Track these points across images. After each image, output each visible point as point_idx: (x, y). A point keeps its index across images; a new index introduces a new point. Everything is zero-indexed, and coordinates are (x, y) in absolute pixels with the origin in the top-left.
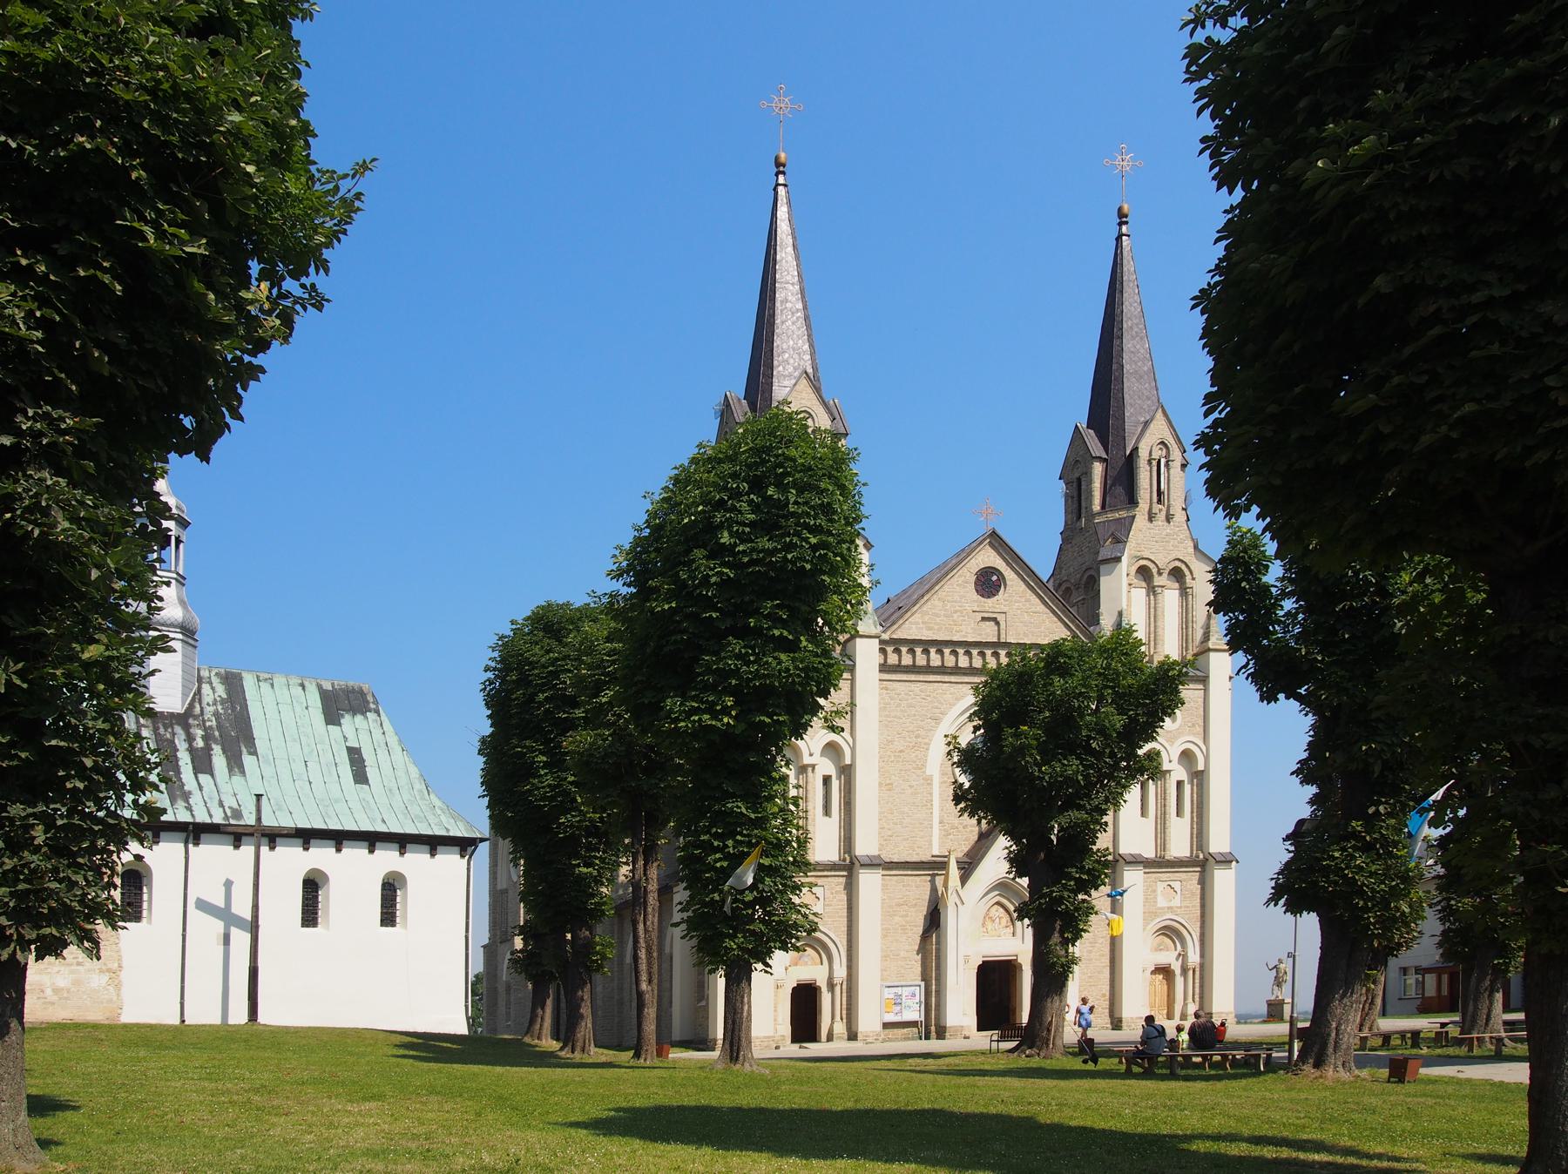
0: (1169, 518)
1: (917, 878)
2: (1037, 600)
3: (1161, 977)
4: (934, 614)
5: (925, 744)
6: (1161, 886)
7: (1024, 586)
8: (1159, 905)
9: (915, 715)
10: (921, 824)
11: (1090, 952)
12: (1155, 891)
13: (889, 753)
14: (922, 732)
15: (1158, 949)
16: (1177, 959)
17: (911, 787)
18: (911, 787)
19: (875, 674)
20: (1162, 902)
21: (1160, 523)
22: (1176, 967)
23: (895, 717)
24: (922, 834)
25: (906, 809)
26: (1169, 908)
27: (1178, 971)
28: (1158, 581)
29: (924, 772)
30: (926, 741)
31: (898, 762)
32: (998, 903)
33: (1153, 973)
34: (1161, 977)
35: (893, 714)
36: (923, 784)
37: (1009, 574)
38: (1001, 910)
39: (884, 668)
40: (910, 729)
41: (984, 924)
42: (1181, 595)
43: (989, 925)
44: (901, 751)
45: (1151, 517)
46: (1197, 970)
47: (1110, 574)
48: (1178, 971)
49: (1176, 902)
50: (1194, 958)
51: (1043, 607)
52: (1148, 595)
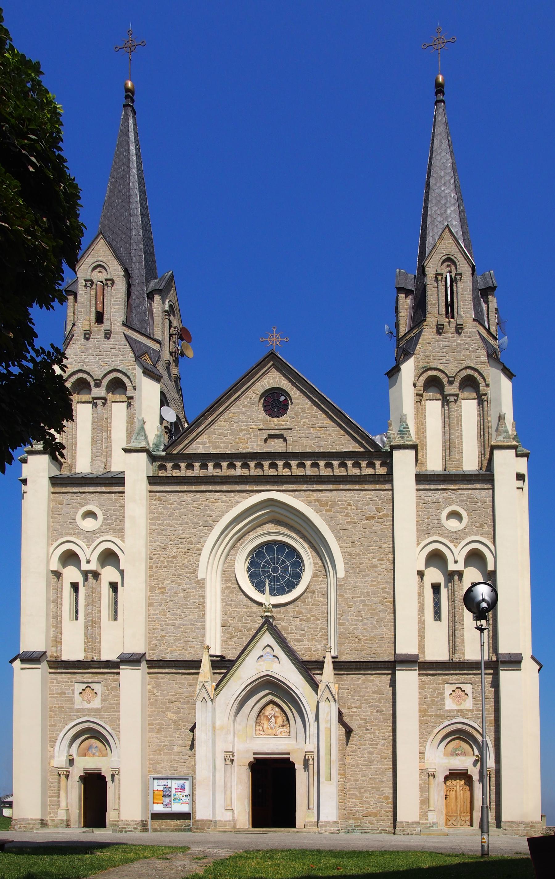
0: (459, 329)
1: (189, 676)
2: (324, 415)
3: (463, 782)
4: (222, 434)
5: (197, 549)
6: (448, 689)
7: (309, 403)
8: (447, 708)
9: (187, 523)
10: (194, 625)
11: (371, 753)
12: (442, 693)
13: (162, 559)
14: (194, 539)
15: (455, 754)
16: (475, 764)
17: (184, 590)
18: (184, 590)
19: (144, 485)
20: (450, 705)
21: (450, 335)
22: (474, 772)
23: (168, 525)
24: (195, 634)
25: (179, 612)
26: (458, 711)
27: (476, 777)
28: (450, 390)
29: (196, 576)
30: (199, 546)
31: (172, 567)
32: (272, 702)
33: (447, 778)
34: (463, 782)
35: (165, 523)
36: (195, 588)
37: (294, 393)
38: (277, 709)
39: (152, 480)
40: (183, 536)
41: (258, 723)
42: (479, 404)
43: (266, 725)
44: (174, 557)
45: (440, 329)
46: (493, 776)
47: (395, 385)
48: (476, 777)
49: (468, 704)
50: (491, 763)
51: (329, 421)
52: (443, 406)
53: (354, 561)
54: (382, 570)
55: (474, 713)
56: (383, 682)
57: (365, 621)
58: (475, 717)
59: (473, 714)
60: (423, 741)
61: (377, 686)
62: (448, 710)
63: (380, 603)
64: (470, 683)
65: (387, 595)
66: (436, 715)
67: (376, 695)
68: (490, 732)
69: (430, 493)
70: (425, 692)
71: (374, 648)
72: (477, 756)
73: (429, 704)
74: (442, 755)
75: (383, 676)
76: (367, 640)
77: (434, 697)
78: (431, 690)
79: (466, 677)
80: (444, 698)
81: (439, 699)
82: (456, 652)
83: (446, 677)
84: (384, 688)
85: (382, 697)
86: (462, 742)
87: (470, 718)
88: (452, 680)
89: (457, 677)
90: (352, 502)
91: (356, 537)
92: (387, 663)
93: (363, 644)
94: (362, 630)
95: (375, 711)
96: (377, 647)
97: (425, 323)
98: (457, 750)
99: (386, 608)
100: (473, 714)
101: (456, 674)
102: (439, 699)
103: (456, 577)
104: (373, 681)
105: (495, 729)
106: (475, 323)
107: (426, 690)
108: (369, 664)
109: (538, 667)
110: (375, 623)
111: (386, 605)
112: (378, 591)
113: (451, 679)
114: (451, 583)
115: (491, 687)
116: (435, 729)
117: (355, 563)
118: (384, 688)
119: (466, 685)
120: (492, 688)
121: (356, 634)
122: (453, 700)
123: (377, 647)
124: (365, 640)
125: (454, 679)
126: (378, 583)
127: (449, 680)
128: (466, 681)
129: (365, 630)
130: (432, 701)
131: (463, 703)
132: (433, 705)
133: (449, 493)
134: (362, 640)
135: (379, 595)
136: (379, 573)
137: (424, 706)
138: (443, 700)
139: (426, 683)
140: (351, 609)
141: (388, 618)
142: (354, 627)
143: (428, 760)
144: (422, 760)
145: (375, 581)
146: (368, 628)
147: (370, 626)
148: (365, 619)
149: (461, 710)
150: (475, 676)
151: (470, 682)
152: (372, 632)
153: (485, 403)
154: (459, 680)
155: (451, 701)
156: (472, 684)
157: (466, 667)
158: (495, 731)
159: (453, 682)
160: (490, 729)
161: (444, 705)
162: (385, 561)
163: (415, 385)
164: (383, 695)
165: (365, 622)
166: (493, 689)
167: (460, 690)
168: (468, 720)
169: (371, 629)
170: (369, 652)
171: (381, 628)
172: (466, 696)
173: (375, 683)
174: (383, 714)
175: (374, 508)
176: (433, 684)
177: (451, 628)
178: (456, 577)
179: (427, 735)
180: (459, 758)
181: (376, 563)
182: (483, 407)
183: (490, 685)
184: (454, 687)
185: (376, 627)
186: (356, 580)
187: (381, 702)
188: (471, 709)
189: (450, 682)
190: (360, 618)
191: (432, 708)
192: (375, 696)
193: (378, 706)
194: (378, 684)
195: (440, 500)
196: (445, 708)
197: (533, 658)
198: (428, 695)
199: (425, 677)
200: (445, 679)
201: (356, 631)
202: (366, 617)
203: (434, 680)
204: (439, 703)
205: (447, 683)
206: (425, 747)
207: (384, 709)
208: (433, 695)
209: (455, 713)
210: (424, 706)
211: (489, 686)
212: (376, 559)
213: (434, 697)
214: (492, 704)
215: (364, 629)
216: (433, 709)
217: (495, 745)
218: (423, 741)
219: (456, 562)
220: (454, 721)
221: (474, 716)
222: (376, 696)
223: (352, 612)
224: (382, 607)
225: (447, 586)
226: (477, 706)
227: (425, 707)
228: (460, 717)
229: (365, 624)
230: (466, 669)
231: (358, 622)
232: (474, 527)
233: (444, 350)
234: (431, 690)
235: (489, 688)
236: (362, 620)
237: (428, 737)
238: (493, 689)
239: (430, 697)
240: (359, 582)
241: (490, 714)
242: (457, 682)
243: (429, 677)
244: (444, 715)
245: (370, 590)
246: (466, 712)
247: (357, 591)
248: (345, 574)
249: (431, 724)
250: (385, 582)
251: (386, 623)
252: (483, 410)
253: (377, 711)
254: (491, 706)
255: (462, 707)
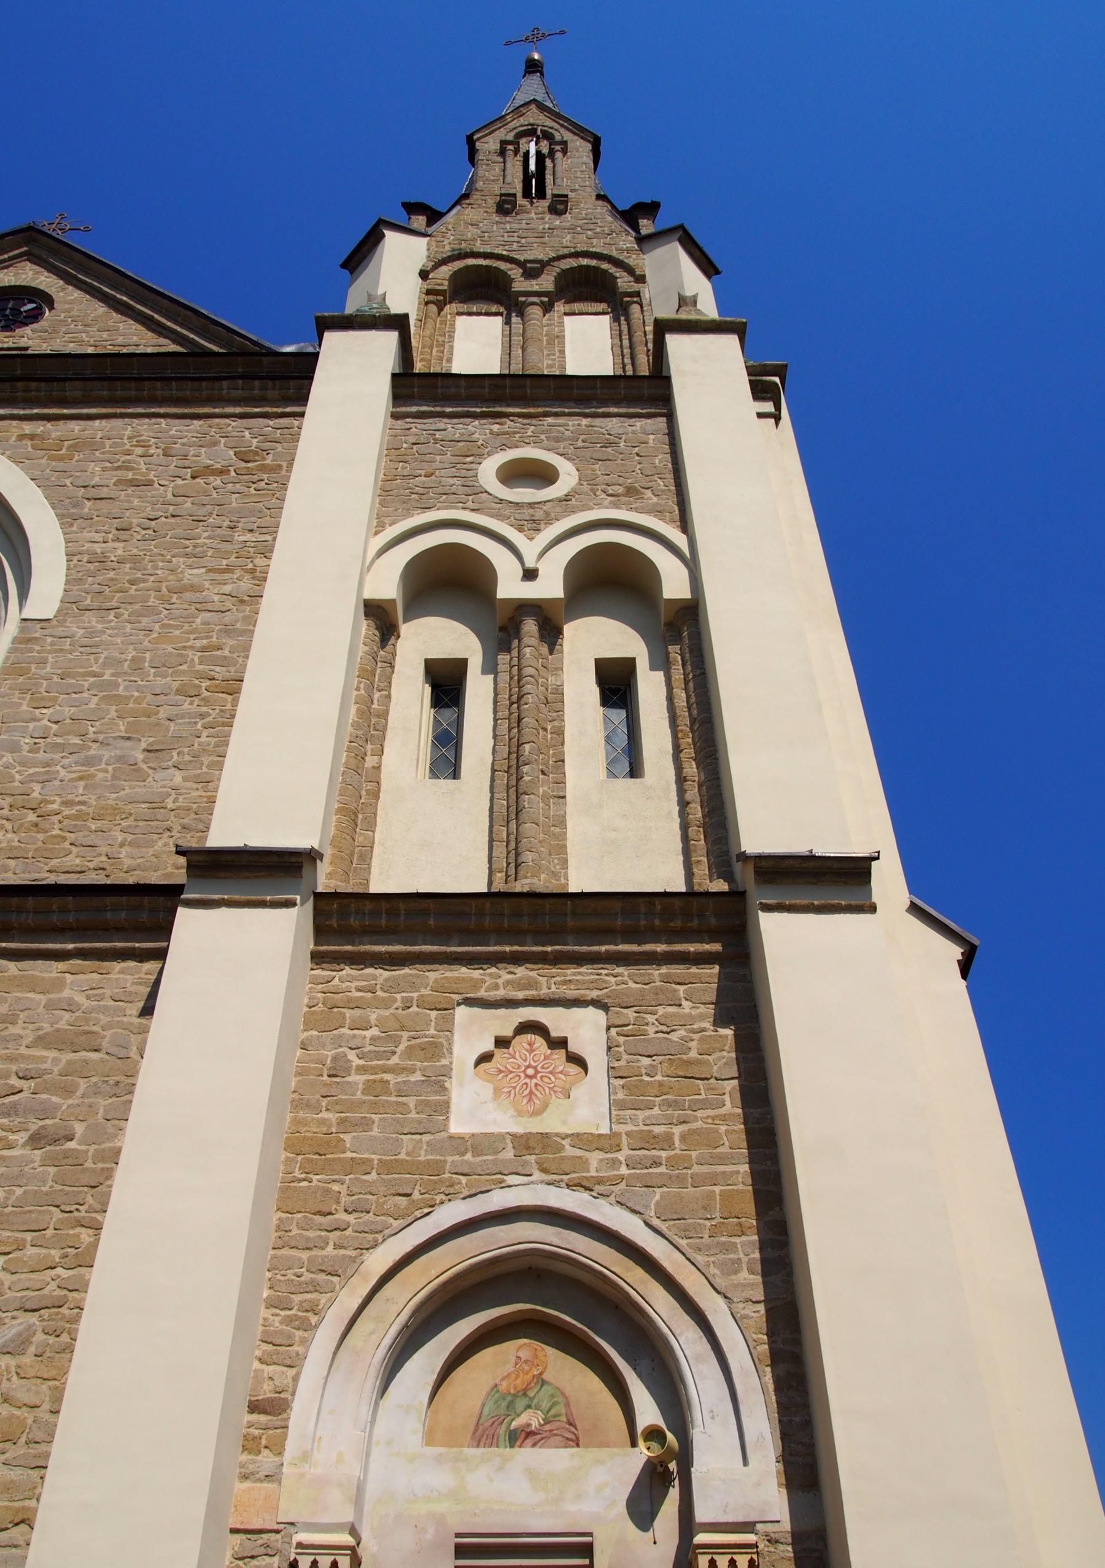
8: (456, 1127)
26: (525, 1143)
53: (112, 574)
54: (216, 598)
55: (621, 1156)
56: (108, 992)
57: (94, 750)
58: (630, 1182)
59: (615, 1163)
60: (288, 1321)
61: (70, 1007)
62: (461, 1138)
63: (179, 692)
64: (597, 1003)
65: (218, 669)
66: (387, 1167)
67: (52, 1054)
68: (733, 1267)
69: (441, 423)
70: (337, 1042)
71: (104, 850)
72: (654, 1434)
73: (359, 1105)
74: (412, 1431)
75: (118, 966)
76: (80, 816)
77: (386, 1070)
78: (374, 1031)
79: (571, 972)
80: (447, 1072)
81: (417, 1077)
82: (521, 873)
83: (463, 971)
84: (104, 1019)
85: (86, 1062)
86: (551, 1352)
87: (600, 1181)
88: (496, 987)
89: (521, 971)
90: (153, 440)
91: (144, 515)
92: (146, 900)
93: (56, 832)
94: (72, 780)
95: (21, 1137)
96: (122, 845)
97: (467, 201)
98: (521, 1403)
99: (204, 709)
100: (615, 1163)
101: (517, 959)
102: (417, 1077)
103: (530, 626)
104: (59, 985)
105: (763, 1246)
106: (600, 203)
107: (345, 1031)
108: (56, 903)
109: (956, 952)
110: (140, 756)
111: (203, 699)
112: (182, 655)
113: (489, 981)
114: (509, 651)
115: (720, 1020)
116: (375, 1246)
117: (112, 579)
118: (104, 1019)
119: (575, 1010)
120: (725, 1025)
121: (35, 795)
122: (497, 1092)
123: (122, 845)
124: (67, 817)
125: (508, 982)
126: (191, 633)
127: (477, 984)
128: (571, 993)
129: (82, 783)
130: (369, 1087)
131: (556, 1102)
132: (375, 1108)
133: (509, 422)
134: (55, 819)
135: (184, 667)
136: (202, 606)
137: (325, 1115)
138: (438, 1081)
139: (350, 1000)
140: (44, 711)
141: (203, 739)
142: (31, 771)
143: (305, 1457)
144: (266, 1460)
145: (177, 627)
146: (101, 775)
147: (110, 768)
148: (95, 746)
149: (545, 1136)
150: (620, 970)
151: (594, 994)
152: (117, 789)
153: (635, 309)
154: (531, 984)
155: (486, 1090)
156: (603, 1006)
157: (570, 922)
158: (764, 1261)
159: (501, 993)
160: (729, 1248)
161: (444, 1108)
162: (238, 573)
163: (424, 275)
164: (94, 1056)
165: (92, 752)
166: (728, 1032)
167: (539, 1042)
168: (585, 1196)
169: (114, 778)
170: (78, 861)
171: (159, 775)
172: (574, 1069)
173: (66, 993)
174: (67, 1154)
175: (232, 453)
176: (386, 1004)
177: (501, 794)
178: (530, 626)
179: (316, 1287)
180: (526, 1455)
181: (195, 581)
182: (628, 320)
183: (710, 1010)
184: (506, 1021)
185: (139, 770)
186: (100, 627)
187: (68, 1091)
188: (604, 1130)
189: (482, 993)
190: (76, 740)
191: (366, 1124)
192: (43, 1059)
193: (46, 1112)
194: (80, 998)
195: (476, 436)
196: (445, 1127)
197: (914, 909)
198: (352, 1056)
199: (348, 971)
200: (457, 980)
201: (37, 787)
202: (101, 737)
203: (391, 987)
204: (411, 1102)
205: (469, 1002)
206: (294, 1363)
207: (79, 1128)
208: (378, 1056)
209: (509, 1154)
210: (325, 1115)
211: (702, 1017)
212: (203, 570)
213: (386, 1070)
214: (731, 1106)
215: (81, 778)
216: (375, 1132)
217: (777, 1358)
218: (288, 1321)
219: (530, 575)
220: (499, 1200)
221: (624, 1171)
222: (53, 1060)
223: (45, 722)
224: (186, 706)
225: (490, 667)
226: (641, 1115)
227: (323, 1122)
228: (537, 1175)
229: (89, 762)
230: (570, 938)
231: (58, 756)
232: (604, 496)
233: (516, 234)
234: (374, 1031)
235: (707, 1025)
236: (83, 747)
237: (324, 1299)
238: (728, 1032)
239: (361, 1070)
240: (109, 632)
241: (722, 1160)
242: (520, 995)
243: (370, 971)
244: (436, 1168)
245: (148, 655)
246: (570, 1151)
247: (92, 657)
248: (59, 611)
249: (351, 1218)
250: (220, 631)
251: (187, 758)
252: (628, 324)
253: (36, 1140)
254: (724, 1118)
255: (552, 1122)
